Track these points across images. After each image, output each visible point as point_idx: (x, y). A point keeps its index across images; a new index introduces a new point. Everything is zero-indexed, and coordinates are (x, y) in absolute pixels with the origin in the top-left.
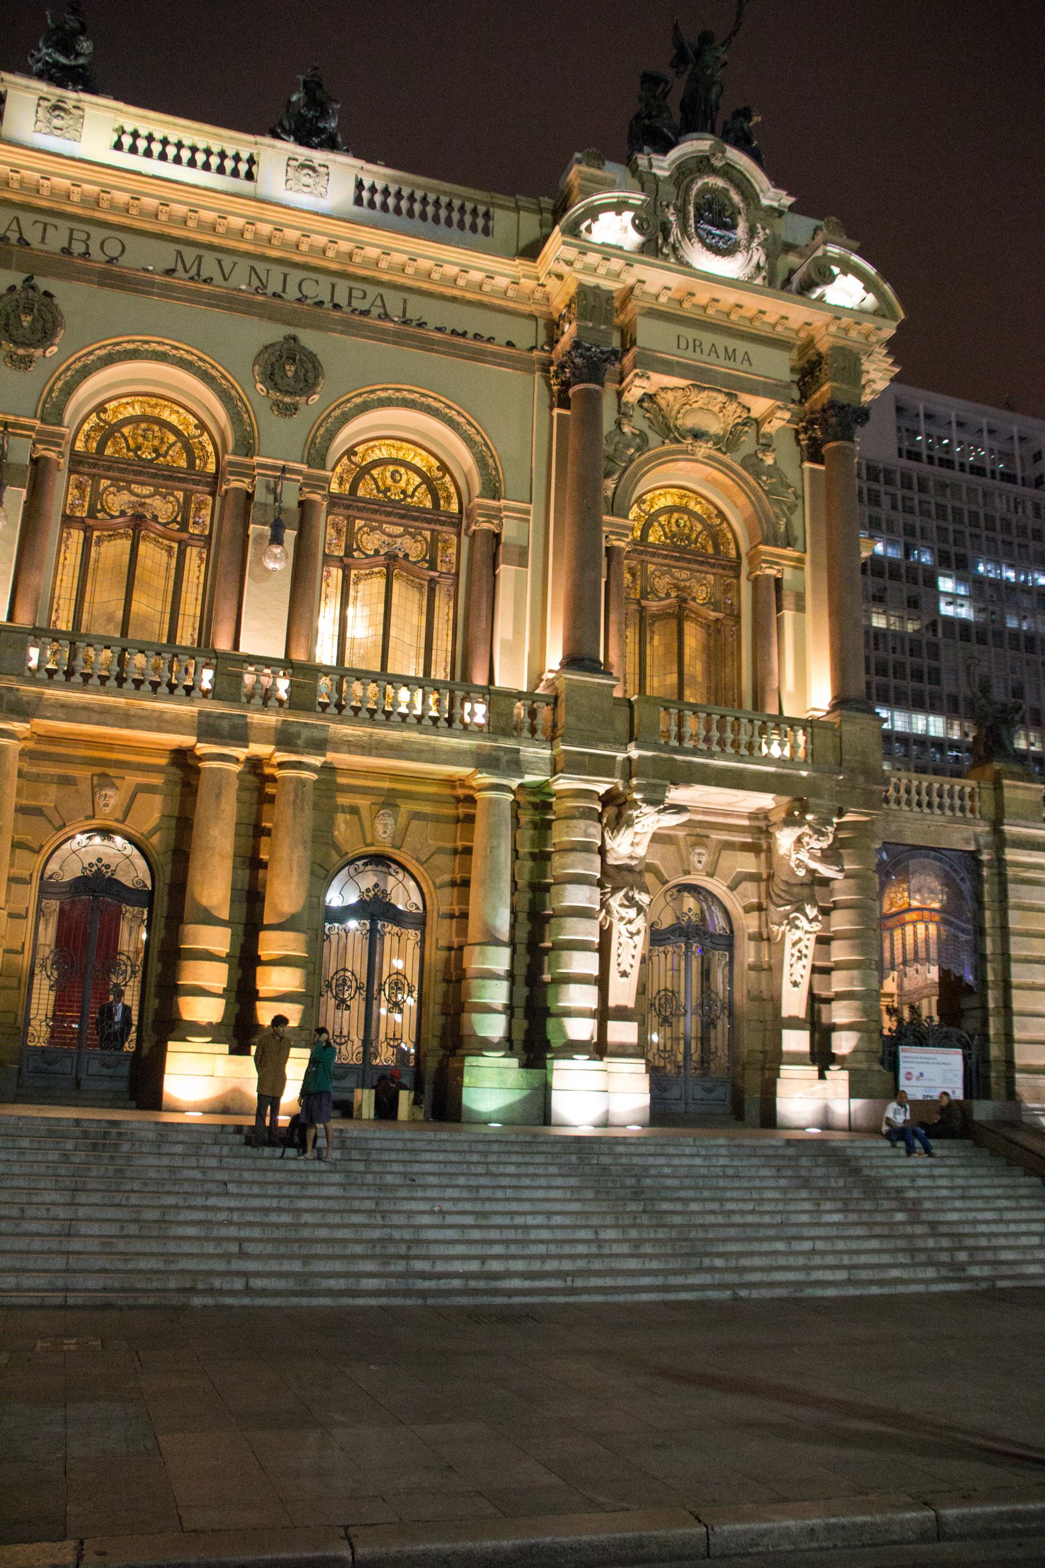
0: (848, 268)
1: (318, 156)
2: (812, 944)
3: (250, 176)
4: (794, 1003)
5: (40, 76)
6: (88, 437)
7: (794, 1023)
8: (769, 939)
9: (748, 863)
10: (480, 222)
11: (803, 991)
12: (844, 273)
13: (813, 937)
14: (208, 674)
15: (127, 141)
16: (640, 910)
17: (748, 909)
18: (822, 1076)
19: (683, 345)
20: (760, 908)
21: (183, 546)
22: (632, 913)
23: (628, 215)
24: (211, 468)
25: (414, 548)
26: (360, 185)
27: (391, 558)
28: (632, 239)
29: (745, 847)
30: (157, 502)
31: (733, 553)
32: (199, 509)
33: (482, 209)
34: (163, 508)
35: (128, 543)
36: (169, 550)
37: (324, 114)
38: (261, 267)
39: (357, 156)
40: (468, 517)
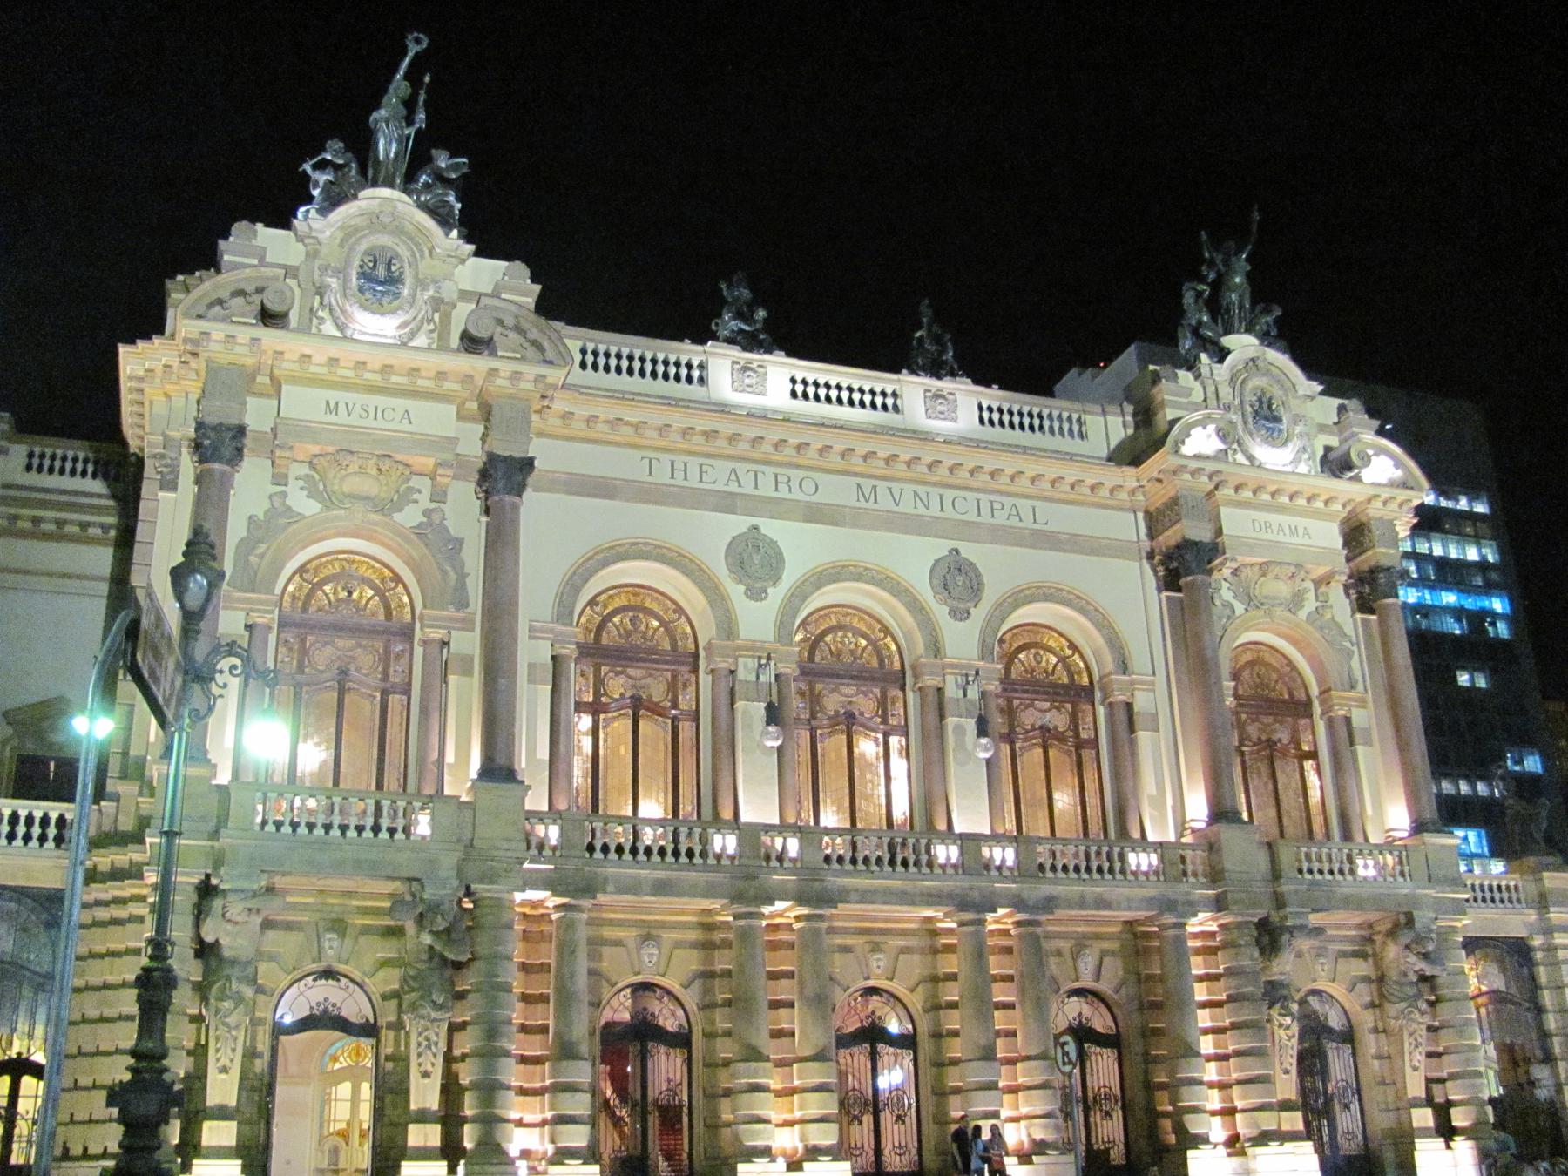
0: (1381, 451)
2: (1424, 1032)
3: (896, 408)
5: (730, 341)
7: (1416, 1103)
8: (1384, 1031)
9: (1362, 968)
10: (1076, 428)
12: (1377, 454)
13: (1424, 1027)
15: (799, 388)
20: (1372, 1005)
21: (886, 735)
22: (1288, 1020)
23: (1211, 428)
24: (897, 665)
26: (980, 408)
27: (1044, 729)
29: (1356, 954)
30: (860, 699)
32: (893, 703)
33: (1075, 416)
35: (844, 737)
36: (876, 740)
38: (921, 490)
39: (976, 382)
40: (1102, 689)
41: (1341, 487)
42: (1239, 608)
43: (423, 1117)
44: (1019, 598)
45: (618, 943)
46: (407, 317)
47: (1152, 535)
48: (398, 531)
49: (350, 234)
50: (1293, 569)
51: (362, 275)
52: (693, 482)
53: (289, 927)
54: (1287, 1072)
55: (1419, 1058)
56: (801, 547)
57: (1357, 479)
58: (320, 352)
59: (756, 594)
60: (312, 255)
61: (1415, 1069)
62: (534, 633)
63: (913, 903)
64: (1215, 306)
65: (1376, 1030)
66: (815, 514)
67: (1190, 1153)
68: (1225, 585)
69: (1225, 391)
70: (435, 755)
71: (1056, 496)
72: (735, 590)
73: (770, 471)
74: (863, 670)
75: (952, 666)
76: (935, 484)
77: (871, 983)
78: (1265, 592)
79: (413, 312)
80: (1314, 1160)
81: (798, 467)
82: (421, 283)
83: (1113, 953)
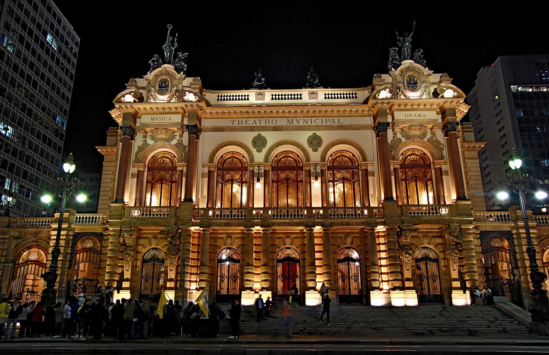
1: (314, 90)
3: (301, 98)
4: (455, 274)
6: (275, 163)
7: (455, 280)
9: (439, 241)
11: (457, 271)
14: (306, 212)
16: (410, 255)
17: (440, 252)
18: (465, 293)
19: (407, 116)
20: (443, 251)
23: (388, 90)
25: (348, 175)
27: (343, 178)
28: (389, 95)
29: (438, 237)
31: (429, 163)
34: (292, 175)
37: (315, 80)
38: (306, 119)
41: (438, 101)
42: (403, 140)
43: (171, 280)
44: (333, 144)
45: (222, 238)
46: (170, 95)
47: (374, 123)
48: (171, 146)
49: (157, 76)
50: (419, 127)
51: (159, 87)
52: (244, 125)
53: (145, 238)
54: (408, 270)
55: (456, 267)
56: (271, 138)
57: (443, 97)
58: (148, 106)
59: (259, 151)
60: (149, 83)
61: (454, 270)
62: (203, 166)
63: (292, 226)
64: (399, 53)
65: (444, 259)
66: (276, 129)
67: (371, 292)
68: (398, 134)
69: (399, 78)
70: (179, 196)
71: (345, 115)
72: (254, 151)
73: (264, 119)
74: (292, 167)
75: (312, 164)
76: (309, 117)
77: (286, 246)
78: (412, 134)
79: (171, 93)
80: (416, 295)
81: (271, 117)
82: (172, 86)
83: (357, 237)
